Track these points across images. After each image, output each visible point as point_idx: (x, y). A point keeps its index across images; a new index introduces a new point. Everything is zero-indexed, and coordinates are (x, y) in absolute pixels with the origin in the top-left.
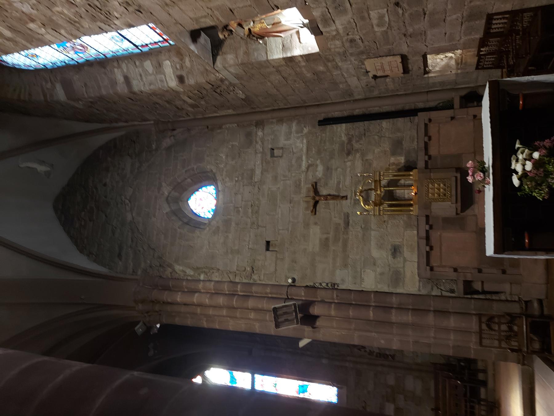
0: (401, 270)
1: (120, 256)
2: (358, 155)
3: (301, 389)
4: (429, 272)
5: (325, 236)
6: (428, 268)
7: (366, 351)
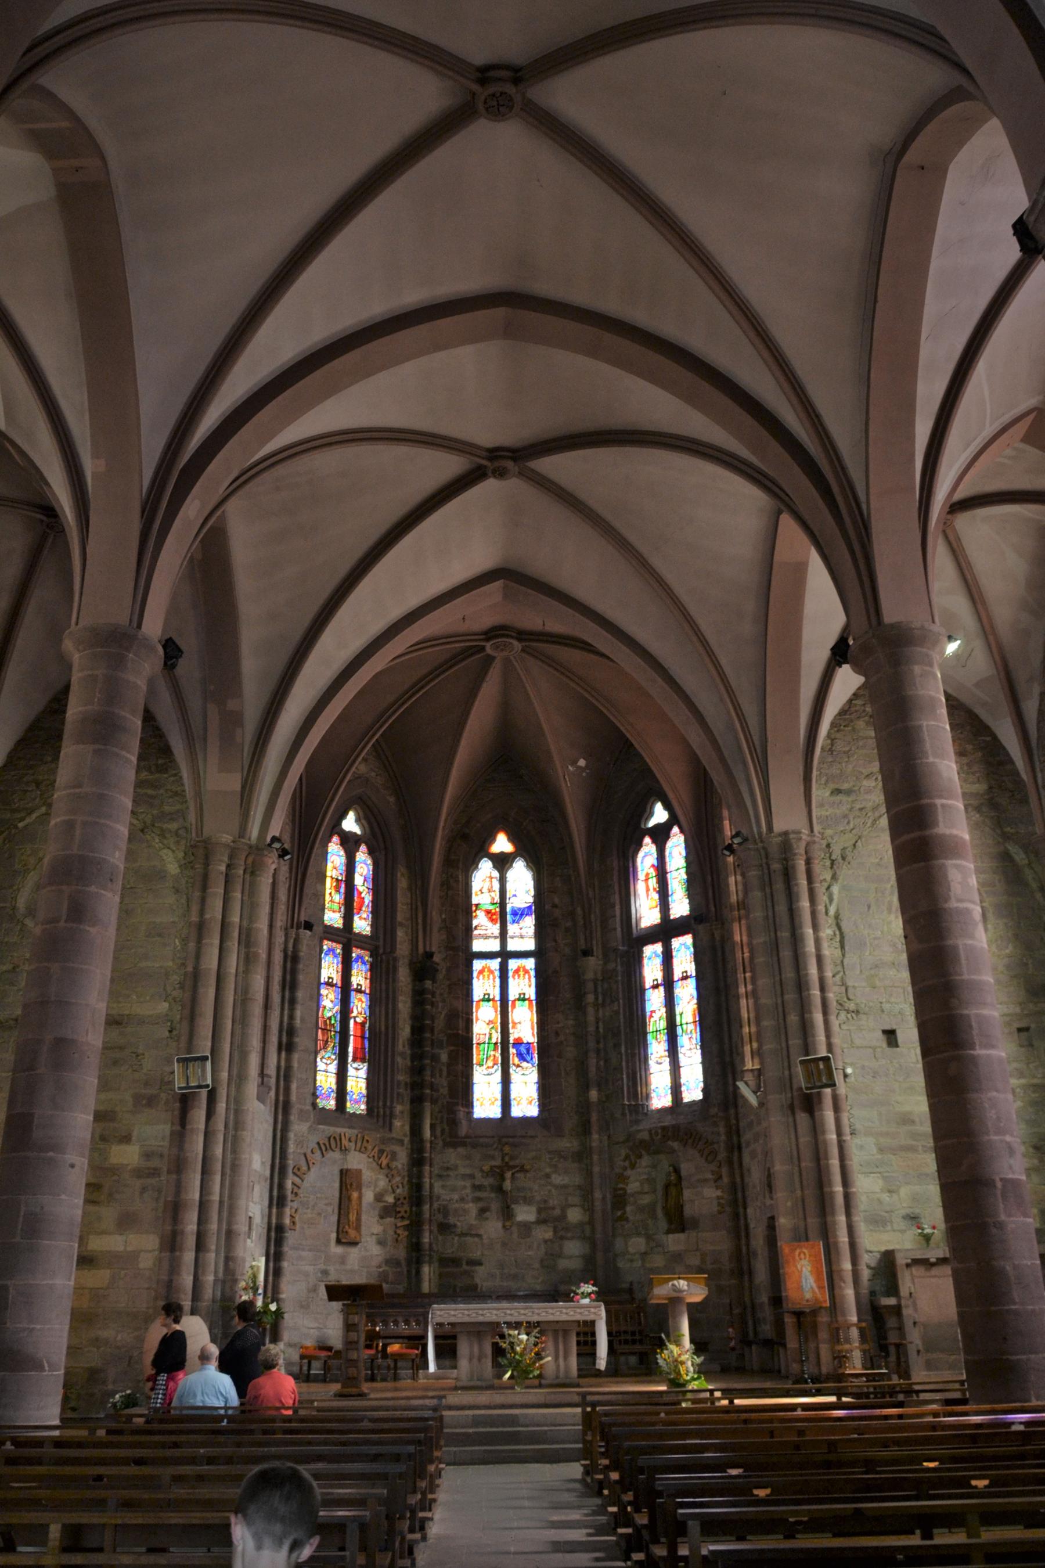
0: (889, 1228)
1: (837, 792)
2: (1036, 1161)
3: (523, 1050)
4: (904, 1262)
5: (917, 1120)
6: (909, 1261)
7: (625, 1169)
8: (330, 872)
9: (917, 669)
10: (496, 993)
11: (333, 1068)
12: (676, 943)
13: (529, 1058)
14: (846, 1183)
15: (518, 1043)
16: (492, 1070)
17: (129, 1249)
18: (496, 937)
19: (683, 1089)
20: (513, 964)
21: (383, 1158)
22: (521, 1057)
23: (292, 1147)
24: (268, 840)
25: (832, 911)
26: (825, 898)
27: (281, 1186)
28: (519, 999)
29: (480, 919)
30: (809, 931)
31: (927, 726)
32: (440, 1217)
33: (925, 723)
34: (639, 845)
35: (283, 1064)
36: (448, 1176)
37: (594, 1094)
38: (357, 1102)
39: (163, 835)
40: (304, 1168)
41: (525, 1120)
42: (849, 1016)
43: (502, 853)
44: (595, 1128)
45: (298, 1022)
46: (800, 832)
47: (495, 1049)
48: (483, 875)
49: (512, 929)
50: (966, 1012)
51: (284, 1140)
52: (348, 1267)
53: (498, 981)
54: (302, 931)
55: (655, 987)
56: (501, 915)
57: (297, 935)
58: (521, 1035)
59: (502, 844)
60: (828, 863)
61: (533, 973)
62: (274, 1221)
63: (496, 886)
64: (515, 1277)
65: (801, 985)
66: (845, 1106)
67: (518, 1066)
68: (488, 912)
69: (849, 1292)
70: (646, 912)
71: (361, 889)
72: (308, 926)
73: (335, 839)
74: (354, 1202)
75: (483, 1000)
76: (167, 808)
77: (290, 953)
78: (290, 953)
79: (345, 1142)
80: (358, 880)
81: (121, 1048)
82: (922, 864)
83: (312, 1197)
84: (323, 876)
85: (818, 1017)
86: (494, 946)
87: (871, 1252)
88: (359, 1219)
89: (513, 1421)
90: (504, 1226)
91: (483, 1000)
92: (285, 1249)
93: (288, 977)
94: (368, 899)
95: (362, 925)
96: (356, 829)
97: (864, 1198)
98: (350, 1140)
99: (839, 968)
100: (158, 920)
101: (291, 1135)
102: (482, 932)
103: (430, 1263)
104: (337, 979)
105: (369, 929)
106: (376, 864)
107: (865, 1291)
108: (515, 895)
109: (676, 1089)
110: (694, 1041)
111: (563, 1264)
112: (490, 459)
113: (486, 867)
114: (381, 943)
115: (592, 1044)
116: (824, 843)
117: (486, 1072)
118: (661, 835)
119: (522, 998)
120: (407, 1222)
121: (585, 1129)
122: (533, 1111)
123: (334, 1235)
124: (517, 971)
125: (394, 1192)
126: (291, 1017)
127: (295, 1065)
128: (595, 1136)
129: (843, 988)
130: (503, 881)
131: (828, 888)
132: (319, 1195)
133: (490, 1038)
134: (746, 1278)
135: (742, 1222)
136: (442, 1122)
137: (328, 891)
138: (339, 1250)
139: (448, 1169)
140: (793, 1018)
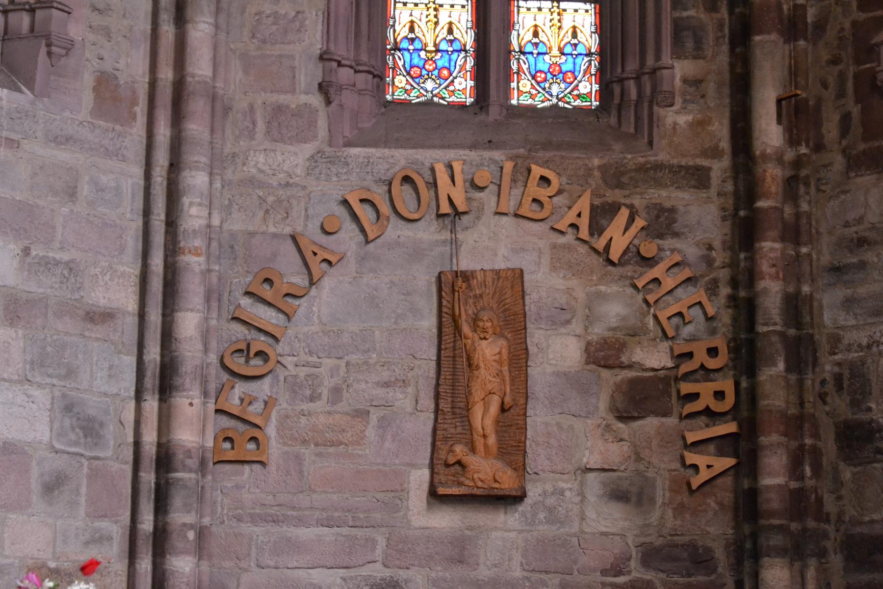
32: (840, 404)
36: (862, 265)
52: (484, 573)
83: (328, 362)
103: (797, 552)
120: (730, 428)
123: (420, 478)
132: (354, 358)
136: (841, 94)
138: (446, 520)
139: (862, 242)
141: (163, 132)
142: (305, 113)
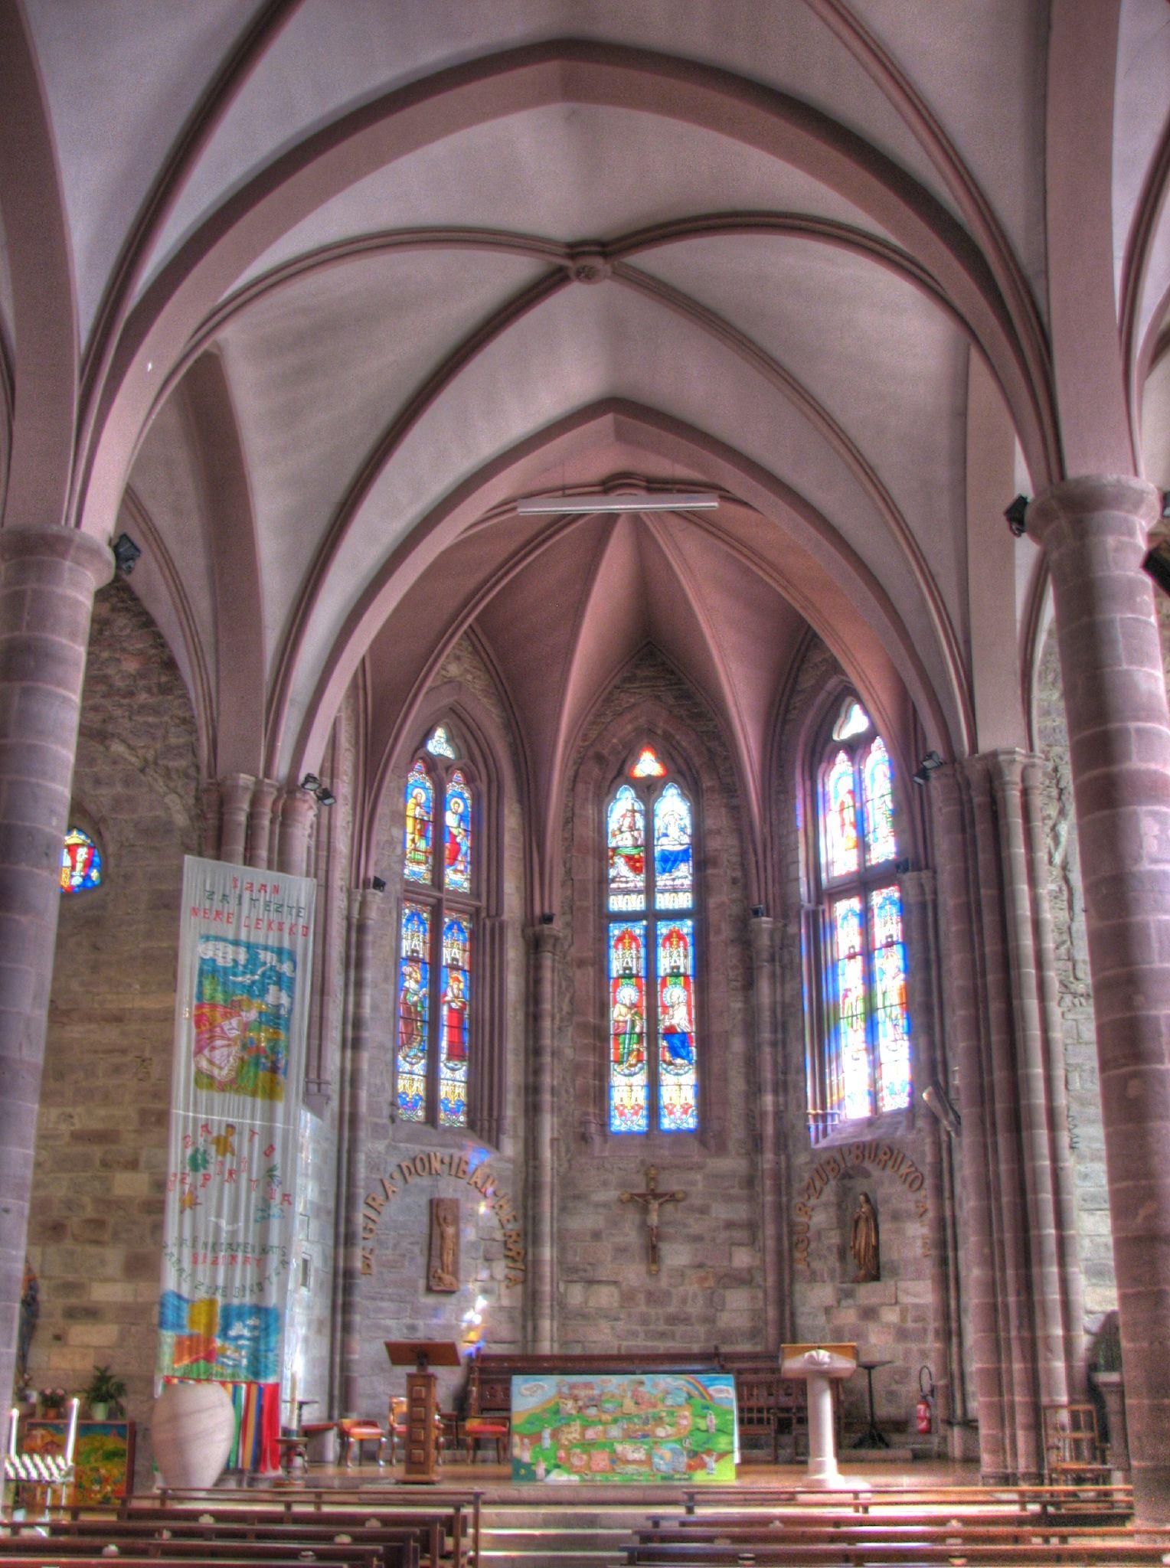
3: (677, 1042)
8: (412, 810)
9: (1111, 541)
10: (638, 966)
11: (420, 1068)
12: (877, 898)
13: (683, 1052)
14: (1060, 1223)
15: (671, 1032)
16: (637, 1069)
17: (140, 1300)
18: (639, 892)
19: (885, 1093)
20: (663, 928)
21: (488, 1185)
22: (676, 1053)
23: (362, 1172)
24: (302, 778)
25: (1058, 859)
26: (1049, 841)
27: (349, 1221)
28: (671, 975)
29: (620, 869)
30: (1023, 888)
31: (1122, 620)
33: (1118, 616)
34: (831, 760)
35: (348, 1065)
37: (768, 1100)
38: (454, 1112)
39: (168, 773)
40: (381, 1198)
41: (678, 1134)
42: (1076, 1001)
43: (649, 777)
44: (769, 1144)
45: (367, 1011)
46: (1013, 752)
47: (640, 1041)
48: (623, 805)
49: (662, 880)
50: (1153, 1013)
51: (351, 1162)
53: (642, 951)
54: (372, 890)
55: (851, 957)
56: (646, 861)
57: (364, 897)
58: (674, 1022)
59: (648, 765)
60: (1055, 793)
61: (689, 940)
62: (341, 1264)
63: (640, 823)
64: (662, 1335)
65: (1008, 961)
66: (1063, 1121)
67: (670, 1063)
68: (630, 859)
69: (1059, 1365)
70: (839, 856)
71: (455, 831)
72: (379, 884)
73: (419, 765)
74: (449, 1243)
75: (623, 977)
76: (173, 741)
77: (355, 921)
78: (355, 921)
79: (436, 1165)
80: (451, 820)
81: (124, 1052)
82: (1106, 812)
84: (400, 818)
85: (1032, 1004)
86: (636, 903)
87: (1091, 1313)
88: (456, 1262)
89: (592, 1521)
90: (649, 1272)
91: (623, 977)
92: (357, 1298)
93: (353, 953)
94: (465, 845)
95: (457, 878)
96: (449, 753)
97: (1086, 1243)
98: (442, 1162)
99: (1065, 937)
100: (163, 887)
101: (362, 1157)
102: (623, 885)
104: (423, 953)
105: (466, 885)
106: (476, 798)
107: (1080, 1364)
108: (666, 835)
109: (874, 1095)
110: (900, 1030)
111: (725, 1320)
112: (572, 257)
113: (625, 801)
114: (484, 903)
115: (766, 1035)
116: (1050, 765)
117: (627, 1072)
118: (857, 748)
119: (675, 974)
121: (756, 1143)
122: (691, 1122)
123: (422, 1283)
124: (668, 938)
125: (503, 1227)
126: (358, 1005)
127: (365, 1066)
128: (769, 1155)
129: (1070, 964)
130: (649, 816)
131: (1053, 828)
133: (633, 1027)
134: (954, 1340)
135: (951, 1268)
137: (409, 837)
140: (995, 1007)
141: (346, 1135)
142: (384, 1126)
